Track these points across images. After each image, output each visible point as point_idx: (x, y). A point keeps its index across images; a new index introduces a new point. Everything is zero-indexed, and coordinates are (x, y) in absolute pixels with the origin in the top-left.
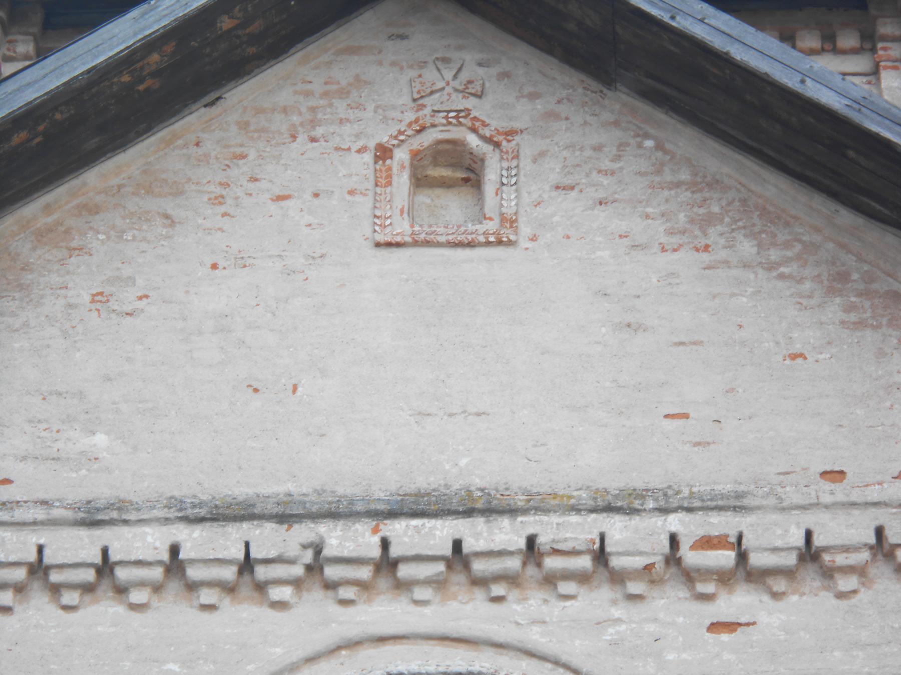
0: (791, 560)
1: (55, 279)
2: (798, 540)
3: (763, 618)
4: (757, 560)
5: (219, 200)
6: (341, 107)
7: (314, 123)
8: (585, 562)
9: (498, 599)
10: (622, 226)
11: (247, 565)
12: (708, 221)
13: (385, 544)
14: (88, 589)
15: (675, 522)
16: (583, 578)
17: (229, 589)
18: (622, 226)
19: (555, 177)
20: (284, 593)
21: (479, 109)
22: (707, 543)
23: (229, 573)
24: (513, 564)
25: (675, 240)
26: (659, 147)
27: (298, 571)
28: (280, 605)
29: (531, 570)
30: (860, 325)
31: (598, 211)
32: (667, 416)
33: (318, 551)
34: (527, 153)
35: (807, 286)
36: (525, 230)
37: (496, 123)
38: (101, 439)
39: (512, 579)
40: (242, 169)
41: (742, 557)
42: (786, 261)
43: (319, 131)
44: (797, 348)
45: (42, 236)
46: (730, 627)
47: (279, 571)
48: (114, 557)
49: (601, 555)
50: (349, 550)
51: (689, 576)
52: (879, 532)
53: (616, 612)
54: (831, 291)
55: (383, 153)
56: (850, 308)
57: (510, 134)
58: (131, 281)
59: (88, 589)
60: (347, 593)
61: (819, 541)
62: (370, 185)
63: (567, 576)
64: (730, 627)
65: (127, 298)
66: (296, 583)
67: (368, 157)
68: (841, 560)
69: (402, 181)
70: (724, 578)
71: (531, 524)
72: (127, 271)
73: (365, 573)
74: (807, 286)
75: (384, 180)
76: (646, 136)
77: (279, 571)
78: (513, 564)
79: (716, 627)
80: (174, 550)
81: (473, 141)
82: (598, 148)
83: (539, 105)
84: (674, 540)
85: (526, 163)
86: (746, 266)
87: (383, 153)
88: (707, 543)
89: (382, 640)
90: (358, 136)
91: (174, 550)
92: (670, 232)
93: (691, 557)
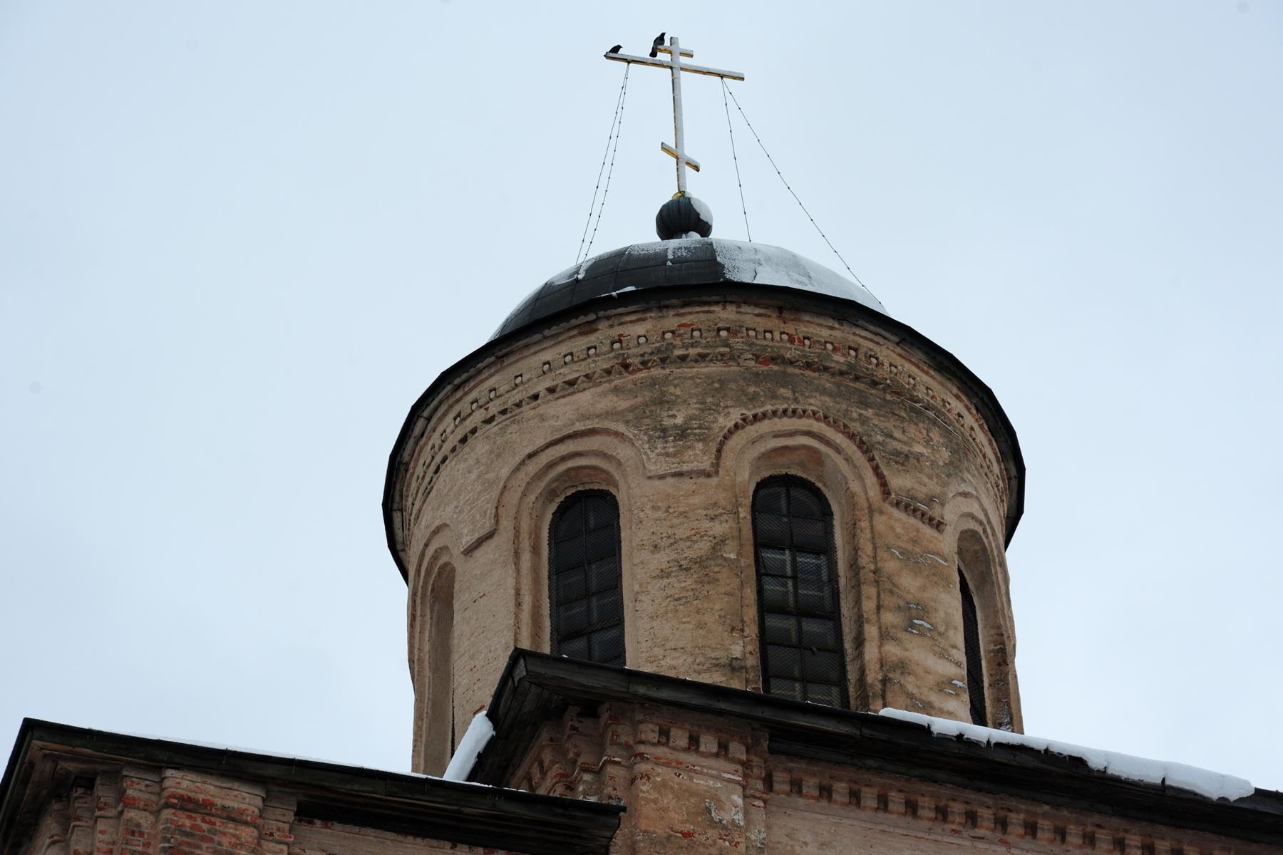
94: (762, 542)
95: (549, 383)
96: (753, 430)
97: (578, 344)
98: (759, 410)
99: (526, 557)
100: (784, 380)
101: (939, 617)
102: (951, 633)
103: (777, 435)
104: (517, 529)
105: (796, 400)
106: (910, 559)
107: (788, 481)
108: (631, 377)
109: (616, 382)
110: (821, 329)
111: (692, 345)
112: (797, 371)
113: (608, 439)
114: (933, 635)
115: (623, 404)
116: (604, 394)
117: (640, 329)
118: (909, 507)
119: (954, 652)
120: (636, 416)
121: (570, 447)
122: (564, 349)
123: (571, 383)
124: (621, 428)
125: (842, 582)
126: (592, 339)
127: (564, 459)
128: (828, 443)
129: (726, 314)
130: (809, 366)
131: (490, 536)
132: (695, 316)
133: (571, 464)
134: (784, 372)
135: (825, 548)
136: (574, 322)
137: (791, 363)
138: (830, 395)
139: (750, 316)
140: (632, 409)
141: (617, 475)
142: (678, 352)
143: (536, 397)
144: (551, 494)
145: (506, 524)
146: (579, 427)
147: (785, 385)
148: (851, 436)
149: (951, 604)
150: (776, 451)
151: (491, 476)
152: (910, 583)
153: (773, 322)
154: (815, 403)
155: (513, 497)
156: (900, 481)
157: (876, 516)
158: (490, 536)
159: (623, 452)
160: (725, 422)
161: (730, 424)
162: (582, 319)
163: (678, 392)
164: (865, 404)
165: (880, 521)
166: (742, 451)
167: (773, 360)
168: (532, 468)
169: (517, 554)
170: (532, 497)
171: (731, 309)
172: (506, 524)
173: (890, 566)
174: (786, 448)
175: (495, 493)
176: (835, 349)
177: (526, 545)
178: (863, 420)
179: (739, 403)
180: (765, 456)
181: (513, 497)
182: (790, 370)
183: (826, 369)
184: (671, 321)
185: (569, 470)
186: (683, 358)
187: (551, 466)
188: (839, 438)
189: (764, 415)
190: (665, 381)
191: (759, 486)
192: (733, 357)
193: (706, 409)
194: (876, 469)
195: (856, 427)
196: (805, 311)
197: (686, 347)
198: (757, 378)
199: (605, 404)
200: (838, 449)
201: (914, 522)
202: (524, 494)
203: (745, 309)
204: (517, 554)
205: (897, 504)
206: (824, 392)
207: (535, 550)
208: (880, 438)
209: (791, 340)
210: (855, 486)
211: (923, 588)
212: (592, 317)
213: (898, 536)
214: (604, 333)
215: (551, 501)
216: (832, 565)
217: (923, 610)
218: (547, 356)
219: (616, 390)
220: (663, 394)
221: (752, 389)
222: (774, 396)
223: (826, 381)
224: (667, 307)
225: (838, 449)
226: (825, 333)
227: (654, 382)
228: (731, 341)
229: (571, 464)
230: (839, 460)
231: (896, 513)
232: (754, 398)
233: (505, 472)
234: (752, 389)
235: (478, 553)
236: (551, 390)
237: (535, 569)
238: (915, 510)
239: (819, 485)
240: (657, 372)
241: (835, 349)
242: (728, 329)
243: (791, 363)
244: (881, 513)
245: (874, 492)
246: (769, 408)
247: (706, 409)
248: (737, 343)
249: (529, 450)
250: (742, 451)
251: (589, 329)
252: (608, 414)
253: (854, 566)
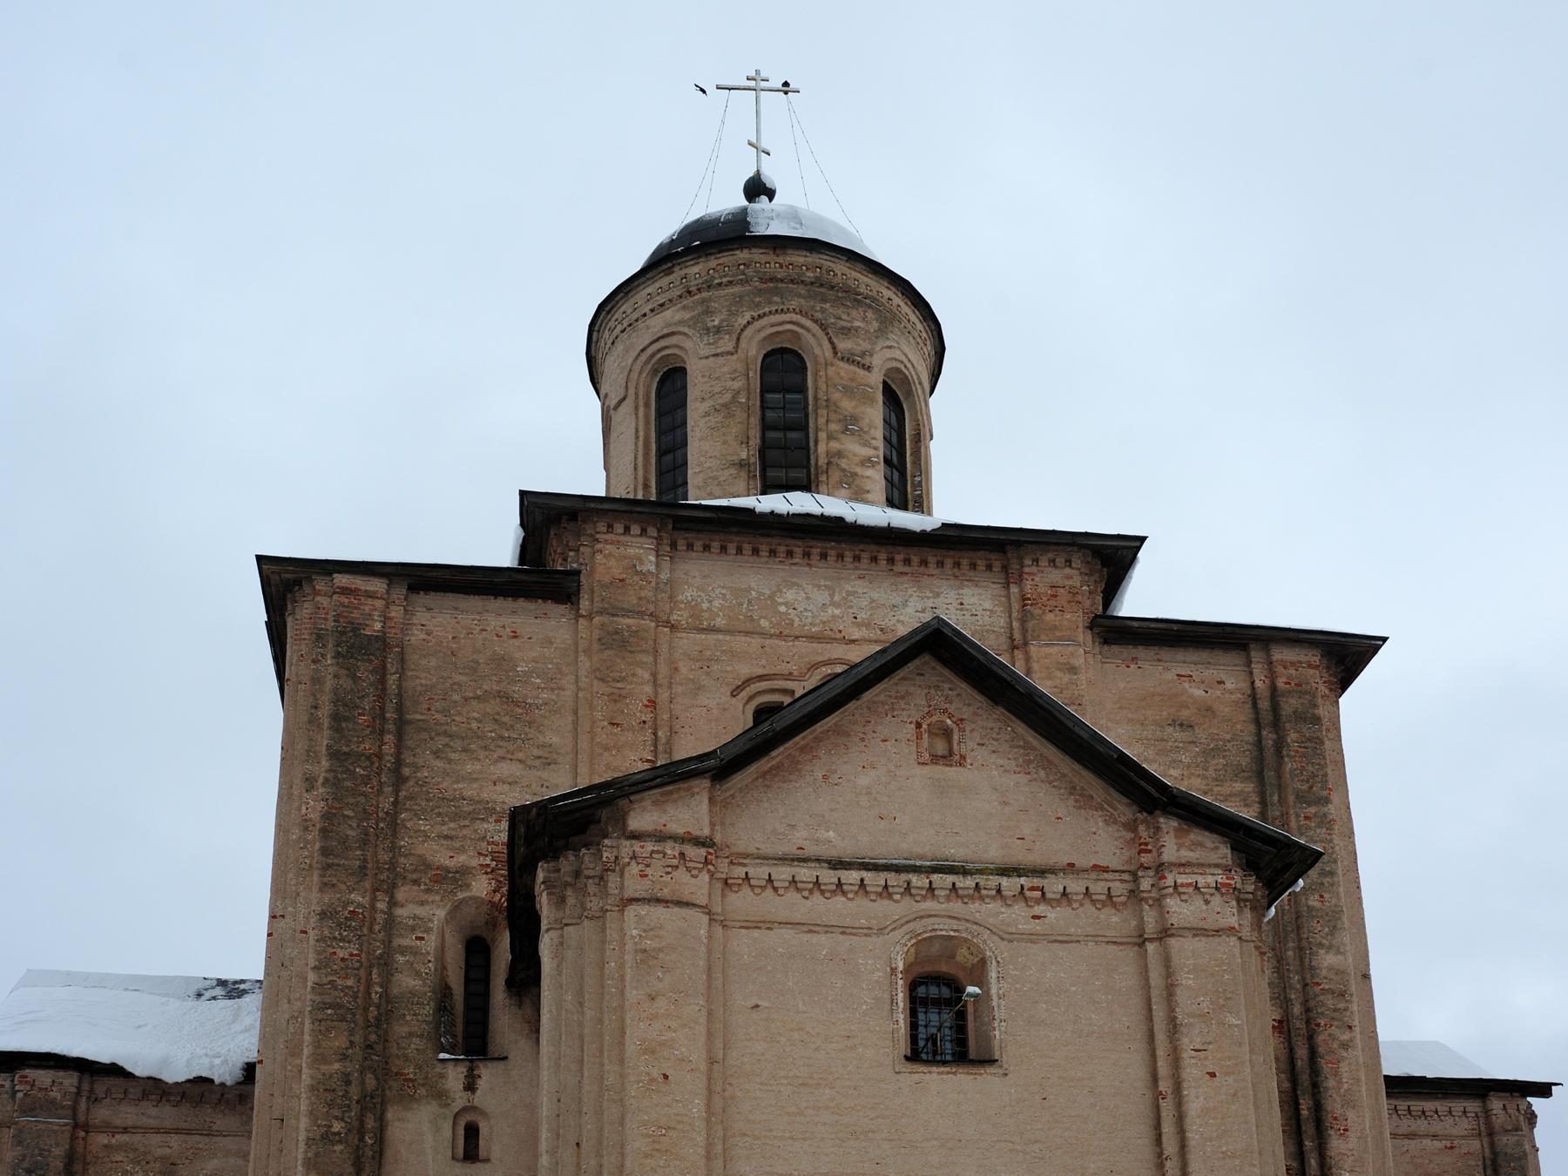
0: (1059, 896)
1: (808, 768)
2: (1061, 888)
3: (1049, 915)
4: (1049, 895)
5: (863, 740)
6: (902, 703)
7: (893, 710)
8: (994, 892)
9: (966, 903)
10: (1001, 762)
11: (886, 887)
12: (1029, 762)
13: (930, 882)
14: (833, 892)
15: (1023, 880)
16: (993, 898)
17: (880, 895)
18: (1001, 762)
19: (978, 740)
20: (897, 897)
21: (952, 708)
22: (1032, 889)
23: (880, 889)
24: (971, 892)
25: (1018, 769)
26: (1013, 731)
27: (902, 890)
28: (897, 901)
29: (976, 894)
30: (1080, 808)
31: (994, 756)
32: (1018, 838)
33: (909, 884)
34: (968, 729)
35: (1062, 791)
36: (969, 761)
37: (958, 715)
38: (831, 833)
39: (971, 897)
40: (869, 728)
41: (1043, 894)
42: (1055, 780)
43: (896, 713)
44: (1060, 815)
45: (803, 749)
46: (1038, 917)
47: (896, 890)
48: (843, 881)
49: (999, 891)
50: (919, 884)
51: (1026, 899)
52: (1087, 888)
53: (1003, 910)
54: (1071, 794)
55: (919, 726)
56: (1076, 801)
57: (962, 720)
58: (835, 772)
59: (833, 892)
60: (918, 898)
61: (1068, 890)
62: (915, 738)
63: (988, 896)
64: (1038, 917)
65: (834, 778)
66: (902, 894)
67: (913, 726)
68: (1074, 897)
69: (926, 736)
70: (1038, 902)
71: (979, 879)
72: (834, 767)
73: (924, 892)
74: (1062, 791)
75: (919, 737)
76: (1009, 726)
77: (896, 890)
78: (971, 892)
79: (1034, 917)
80: (862, 880)
81: (949, 722)
82: (992, 729)
83: (971, 709)
84: (1022, 886)
85: (967, 733)
86: (1042, 781)
87: (919, 726)
88: (1032, 889)
89: (930, 916)
90: (909, 716)
91: (862, 880)
92: (1017, 766)
93: (1028, 894)
94: (765, 389)
95: (650, 307)
96: (757, 324)
97: (665, 281)
98: (761, 312)
99: (641, 409)
100: (776, 291)
101: (864, 423)
102: (873, 431)
103: (773, 326)
104: (637, 394)
105: (783, 303)
106: (848, 391)
107: (783, 351)
108: (691, 299)
109: (685, 302)
110: (799, 258)
111: (724, 276)
112: (784, 285)
113: (680, 337)
114: (862, 436)
115: (688, 316)
116: (678, 311)
117: (696, 269)
118: (849, 359)
119: (874, 441)
120: (694, 322)
121: (662, 343)
122: (657, 285)
123: (662, 305)
124: (686, 330)
125: (810, 407)
126: (671, 277)
127: (659, 351)
128: (802, 327)
129: (743, 255)
130: (792, 281)
131: (624, 399)
132: (726, 258)
133: (663, 353)
134: (776, 288)
135: (802, 389)
136: (661, 269)
137: (782, 281)
138: (804, 298)
139: (757, 255)
140: (692, 318)
141: (686, 358)
142: (717, 281)
143: (645, 315)
144: (655, 371)
145: (631, 391)
146: (666, 331)
147: (776, 295)
148: (816, 321)
149: (875, 415)
150: (772, 334)
151: (624, 364)
152: (847, 405)
153: (771, 257)
154: (794, 303)
155: (634, 375)
156: (844, 345)
157: (829, 367)
158: (624, 399)
159: (688, 344)
160: (742, 321)
161: (745, 322)
162: (664, 267)
163: (716, 305)
164: (824, 301)
165: (831, 371)
166: (752, 338)
167: (771, 280)
168: (644, 357)
169: (637, 408)
170: (644, 375)
171: (746, 251)
172: (631, 391)
173: (836, 396)
174: (778, 332)
175: (626, 374)
176: (807, 269)
177: (641, 403)
178: (823, 311)
179: (750, 308)
180: (765, 339)
181: (634, 375)
182: (780, 285)
183: (802, 282)
184: (713, 263)
185: (663, 357)
186: (720, 284)
187: (653, 355)
188: (808, 323)
189: (765, 314)
190: (710, 299)
191: (766, 356)
192: (747, 281)
193: (731, 314)
194: (830, 340)
195: (819, 315)
196: (789, 248)
197: (721, 278)
198: (760, 292)
199: (678, 317)
200: (808, 330)
201: (853, 368)
202: (640, 373)
203: (754, 250)
204: (637, 408)
205: (842, 359)
206: (799, 296)
207: (647, 405)
208: (833, 320)
209: (781, 267)
210: (817, 351)
211: (856, 407)
212: (670, 265)
213: (842, 378)
214: (678, 273)
215: (656, 375)
216: (806, 398)
217: (854, 419)
218: (649, 290)
219: (684, 308)
220: (708, 307)
221: (757, 300)
222: (770, 302)
223: (802, 290)
224: (710, 254)
225: (808, 330)
226: (802, 260)
227: (703, 301)
228: (746, 271)
229: (663, 353)
230: (809, 336)
231: (841, 364)
232: (758, 305)
233: (630, 361)
234: (757, 300)
235: (620, 408)
236: (652, 310)
237: (647, 417)
238: (853, 361)
239: (800, 351)
240: (705, 294)
241: (807, 269)
242: (744, 264)
243: (782, 281)
244: (832, 365)
245: (829, 353)
246: (767, 310)
247: (731, 314)
248: (750, 272)
249: (641, 348)
250: (752, 338)
251: (669, 272)
252: (681, 322)
253: (816, 399)
